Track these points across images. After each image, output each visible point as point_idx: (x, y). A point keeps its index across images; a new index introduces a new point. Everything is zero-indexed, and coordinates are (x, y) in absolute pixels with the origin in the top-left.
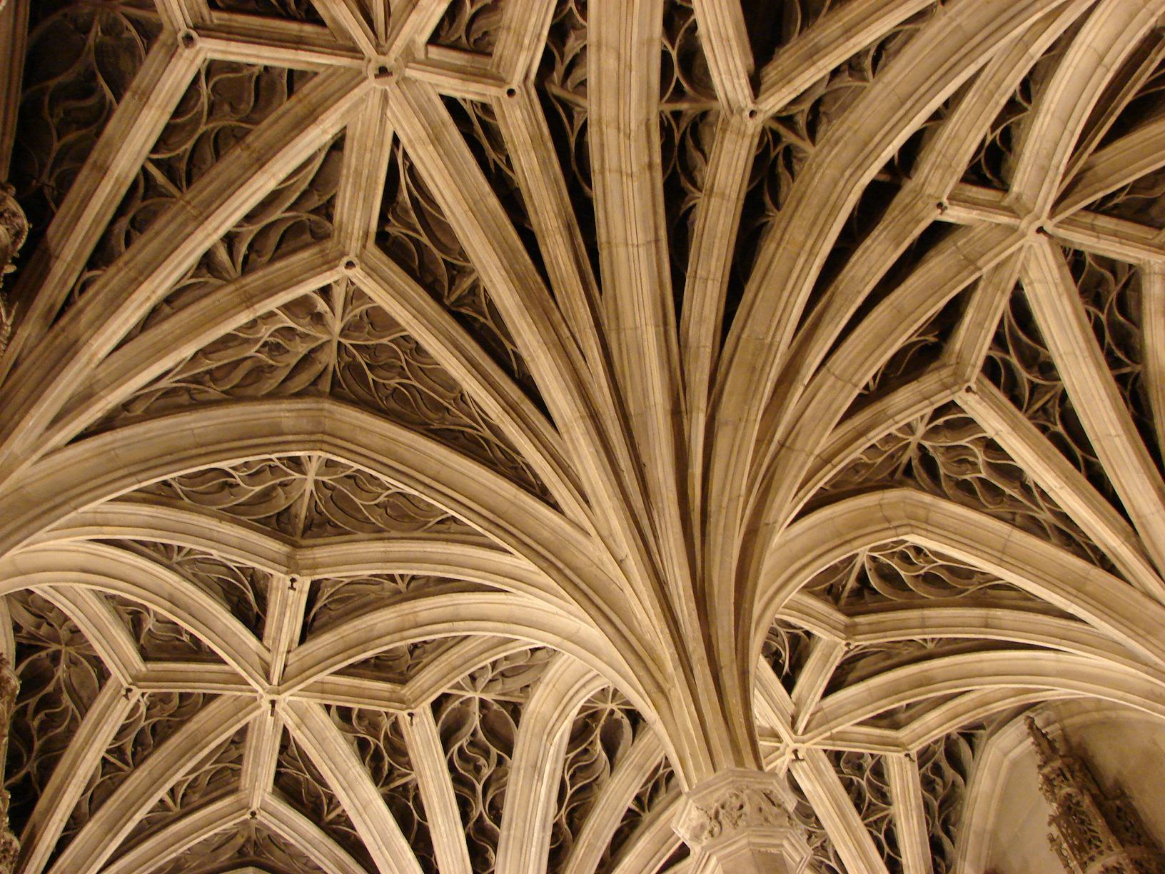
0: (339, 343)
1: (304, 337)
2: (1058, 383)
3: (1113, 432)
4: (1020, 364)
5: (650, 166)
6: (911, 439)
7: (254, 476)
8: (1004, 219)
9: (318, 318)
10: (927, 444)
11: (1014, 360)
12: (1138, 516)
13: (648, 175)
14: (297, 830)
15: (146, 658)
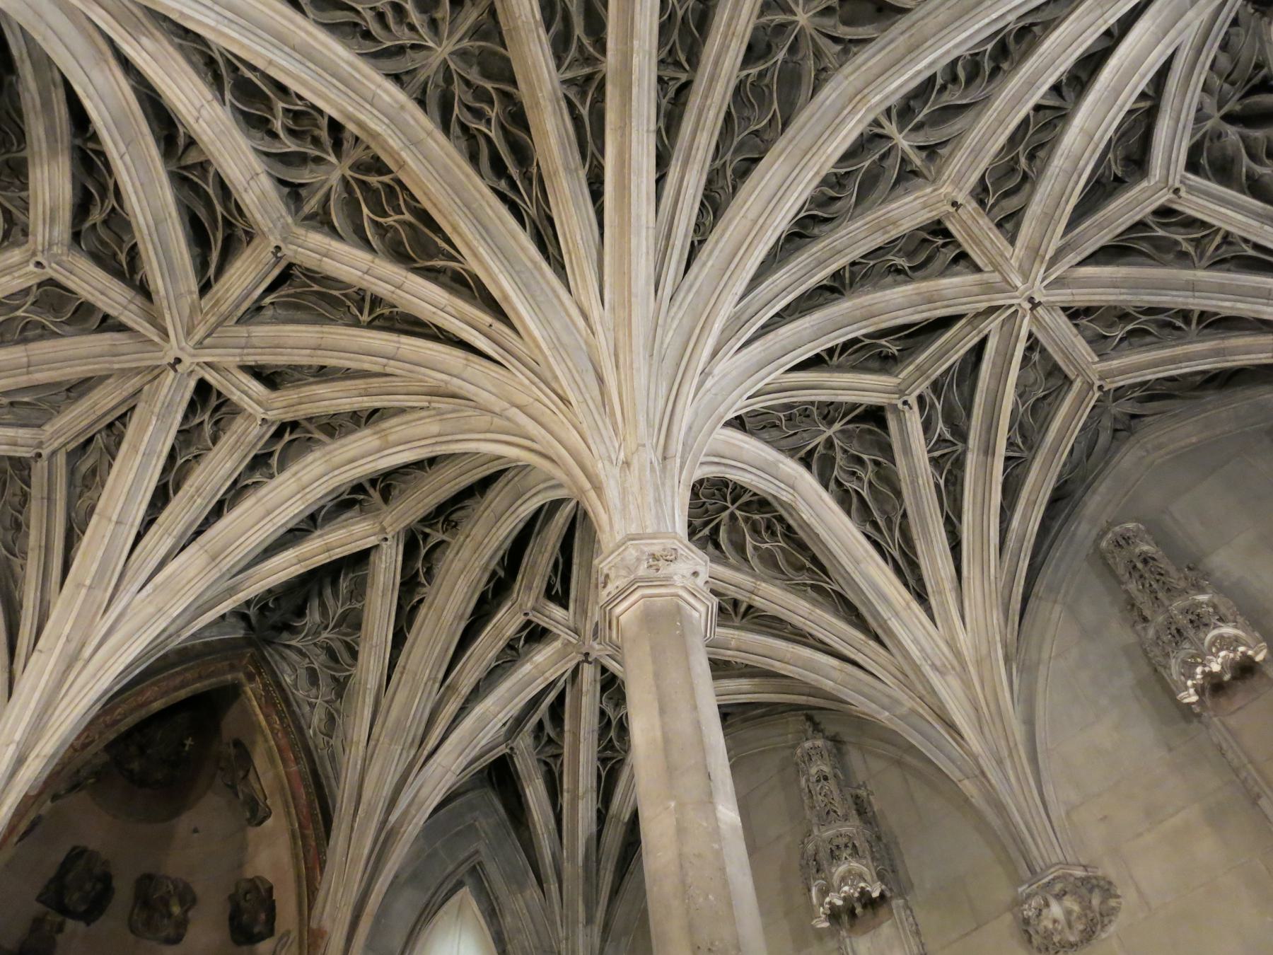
0: (733, 503)
1: (747, 520)
2: (174, 169)
3: (127, 157)
4: (214, 228)
5: (467, 537)
6: (348, 173)
7: (860, 461)
8: (212, 378)
9: (733, 517)
10: (333, 159)
11: (219, 209)
12: (106, 61)
13: (473, 533)
14: (1171, 139)
15: (1068, 381)
